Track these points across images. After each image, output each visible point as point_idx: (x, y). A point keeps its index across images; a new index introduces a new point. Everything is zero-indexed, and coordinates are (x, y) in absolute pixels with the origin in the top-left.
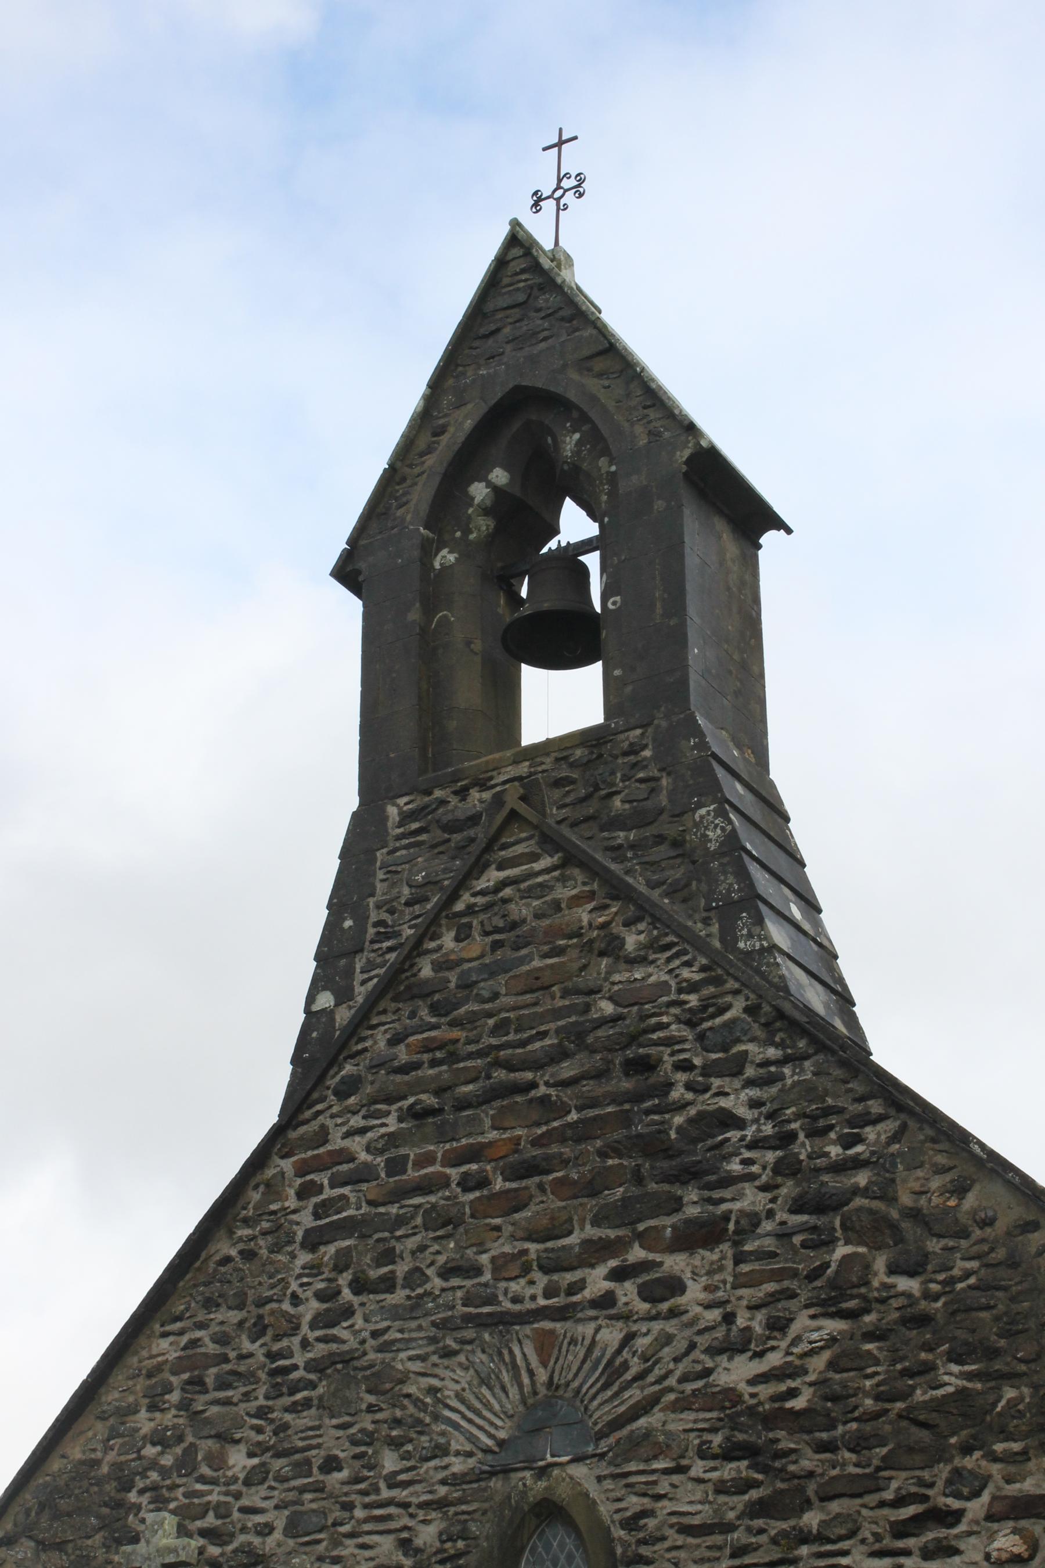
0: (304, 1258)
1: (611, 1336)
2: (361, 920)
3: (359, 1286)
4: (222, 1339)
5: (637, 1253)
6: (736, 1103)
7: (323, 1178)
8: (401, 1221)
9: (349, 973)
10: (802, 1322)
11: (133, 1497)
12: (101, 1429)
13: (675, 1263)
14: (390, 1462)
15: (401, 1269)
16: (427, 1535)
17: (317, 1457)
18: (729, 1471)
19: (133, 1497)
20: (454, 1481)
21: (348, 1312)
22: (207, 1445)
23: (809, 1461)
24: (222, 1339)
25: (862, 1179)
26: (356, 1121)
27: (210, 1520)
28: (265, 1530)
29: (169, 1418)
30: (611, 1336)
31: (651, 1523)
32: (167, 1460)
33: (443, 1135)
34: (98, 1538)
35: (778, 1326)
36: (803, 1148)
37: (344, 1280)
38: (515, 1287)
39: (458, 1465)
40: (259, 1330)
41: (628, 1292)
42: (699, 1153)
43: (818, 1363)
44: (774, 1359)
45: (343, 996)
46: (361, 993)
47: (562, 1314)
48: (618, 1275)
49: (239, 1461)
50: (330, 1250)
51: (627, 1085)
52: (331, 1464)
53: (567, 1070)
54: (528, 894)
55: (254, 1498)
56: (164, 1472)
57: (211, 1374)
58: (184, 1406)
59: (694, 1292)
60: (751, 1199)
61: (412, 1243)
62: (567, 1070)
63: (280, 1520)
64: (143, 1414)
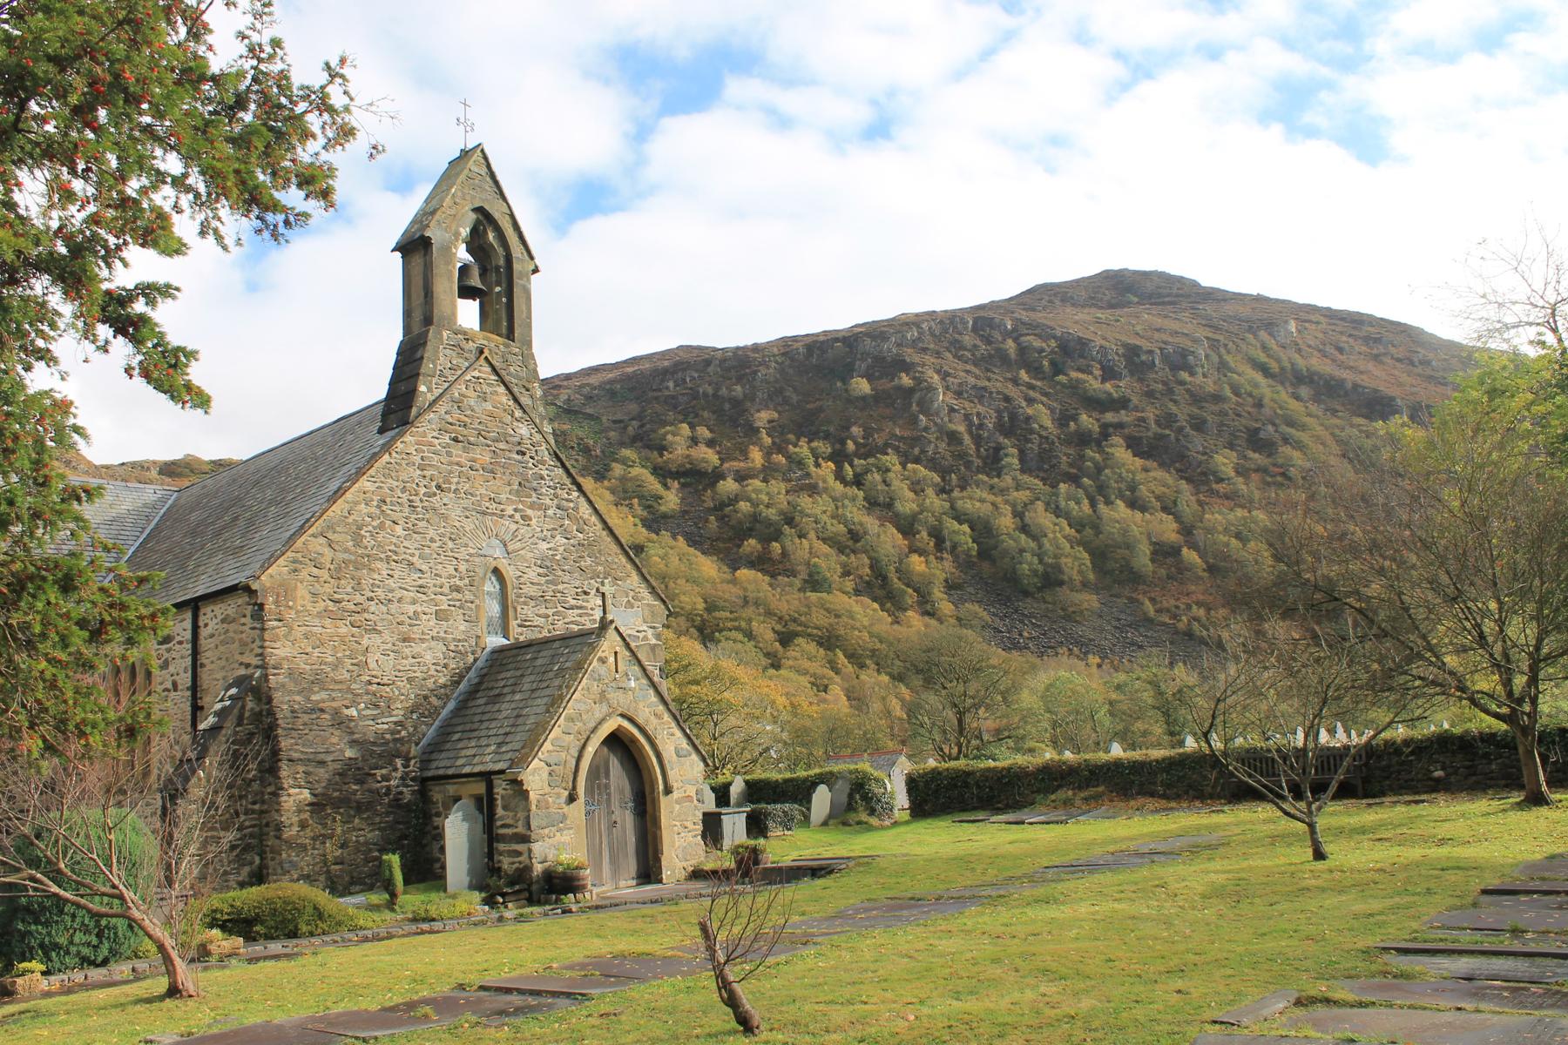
0: (419, 472)
1: (514, 527)
2: (435, 366)
3: (438, 487)
4: (391, 489)
5: (521, 507)
6: (545, 473)
7: (425, 448)
8: (451, 472)
9: (431, 382)
10: (558, 537)
11: (363, 532)
12: (347, 507)
13: (529, 512)
14: (451, 545)
15: (453, 487)
16: (463, 567)
17: (428, 537)
18: (541, 571)
19: (363, 532)
20: (471, 555)
21: (435, 495)
22: (388, 523)
23: (560, 573)
24: (391, 489)
25: (572, 505)
26: (435, 434)
27: (392, 548)
28: (412, 555)
29: (373, 510)
30: (514, 527)
31: (522, 580)
32: (375, 524)
33: (465, 450)
34: (351, 543)
35: (552, 537)
36: (559, 491)
37: (434, 484)
38: (487, 504)
39: (472, 551)
40: (404, 490)
41: (517, 516)
42: (535, 484)
43: (561, 549)
44: (551, 545)
45: (430, 390)
46: (437, 392)
47: (502, 517)
48: (516, 510)
49: (399, 530)
50: (427, 473)
51: (516, 456)
52: (432, 540)
53: (502, 446)
54: (488, 384)
55: (406, 544)
56: (374, 528)
57: (388, 500)
58: (378, 507)
59: (534, 522)
60: (548, 502)
61: (456, 480)
62: (502, 446)
63: (417, 553)
64: (363, 506)
